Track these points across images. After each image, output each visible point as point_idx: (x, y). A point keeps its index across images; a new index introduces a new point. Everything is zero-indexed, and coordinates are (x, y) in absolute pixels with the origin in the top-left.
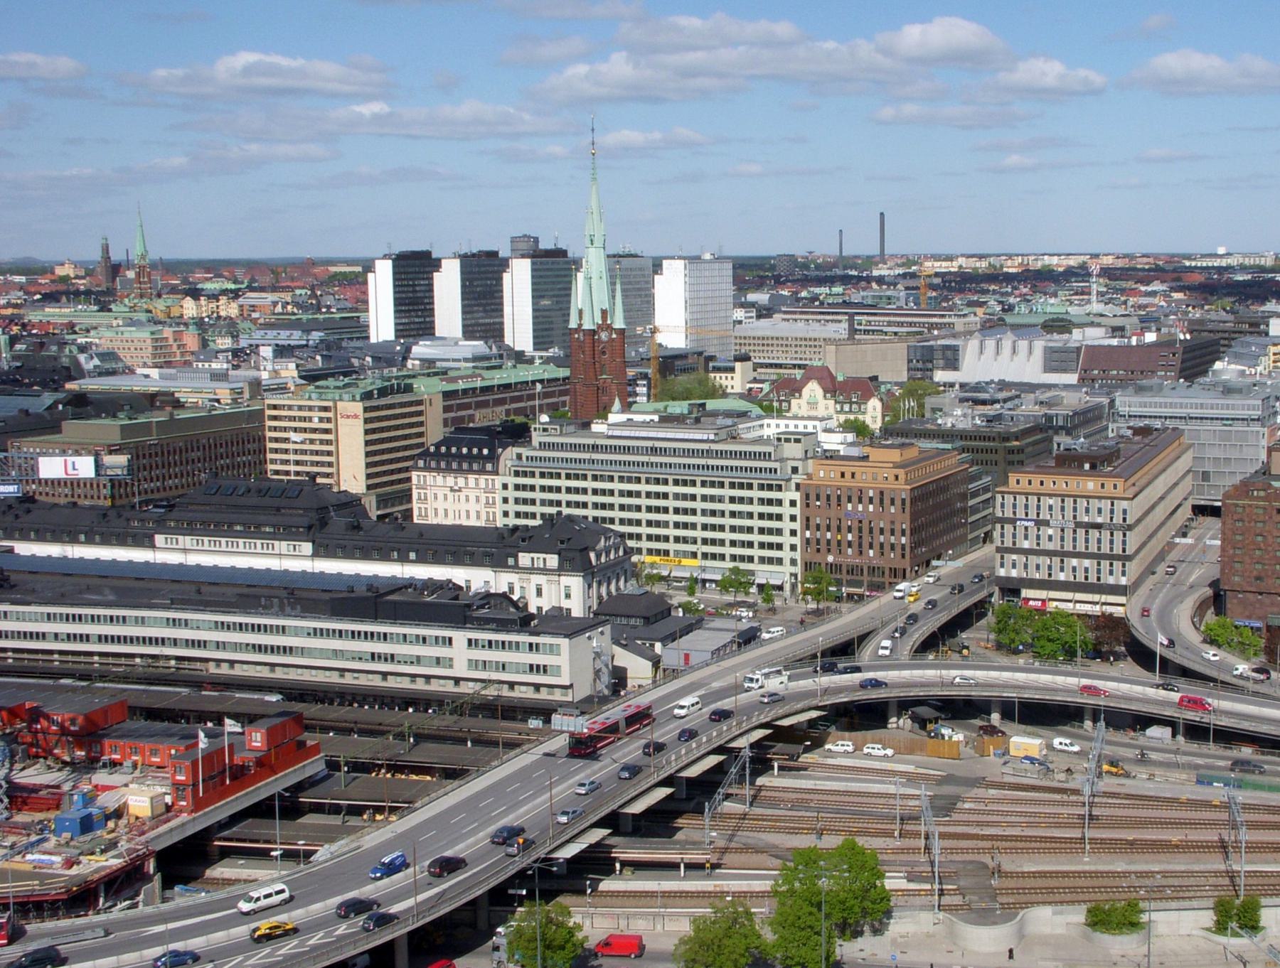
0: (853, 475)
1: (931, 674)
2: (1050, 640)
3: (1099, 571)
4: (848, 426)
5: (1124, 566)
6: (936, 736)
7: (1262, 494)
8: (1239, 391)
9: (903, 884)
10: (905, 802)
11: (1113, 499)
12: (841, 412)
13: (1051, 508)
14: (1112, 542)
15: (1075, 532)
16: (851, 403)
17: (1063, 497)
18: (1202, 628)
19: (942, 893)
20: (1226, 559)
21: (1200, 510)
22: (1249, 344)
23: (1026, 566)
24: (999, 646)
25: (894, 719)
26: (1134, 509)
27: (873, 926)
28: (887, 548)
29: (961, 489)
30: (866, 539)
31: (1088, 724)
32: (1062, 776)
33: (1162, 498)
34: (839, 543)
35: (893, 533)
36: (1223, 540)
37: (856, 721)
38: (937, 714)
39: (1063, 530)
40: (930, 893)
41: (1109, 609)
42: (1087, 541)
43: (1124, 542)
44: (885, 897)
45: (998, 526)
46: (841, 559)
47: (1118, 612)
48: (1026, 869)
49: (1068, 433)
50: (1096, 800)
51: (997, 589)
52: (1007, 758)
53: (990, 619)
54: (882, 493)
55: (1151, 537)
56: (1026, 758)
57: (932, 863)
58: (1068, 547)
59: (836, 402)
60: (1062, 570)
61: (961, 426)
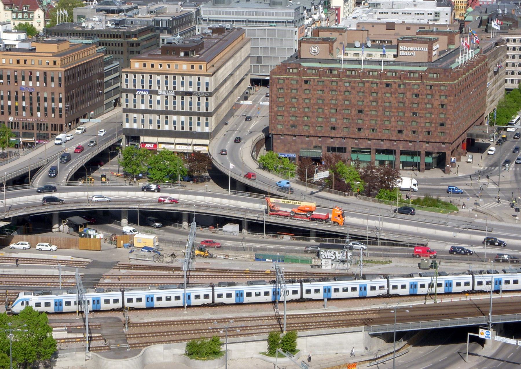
0: (25, 62)
1: (81, 195)
2: (160, 170)
3: (191, 124)
4: (21, 29)
5: (207, 120)
6: (85, 235)
9: (65, 335)
10: (65, 280)
11: (199, 76)
12: (16, 18)
13: (159, 82)
14: (199, 104)
15: (175, 98)
16: (23, 13)
17: (167, 75)
18: (258, 159)
19: (91, 339)
20: (273, 114)
21: (256, 82)
23: (143, 121)
24: (126, 175)
25: (56, 226)
26: (213, 82)
27: (45, 363)
28: (49, 111)
29: (99, 70)
30: (35, 106)
31: (185, 224)
32: (169, 259)
33: (231, 75)
34: (17, 108)
35: (53, 100)
36: (271, 102)
37: (31, 228)
38: (86, 221)
39: (167, 97)
40: (83, 339)
41: (198, 149)
42: (183, 104)
43: (207, 104)
44: (53, 344)
45: (124, 95)
46: (18, 119)
47: (204, 150)
48: (146, 321)
49: (170, 32)
50: (191, 273)
51: (124, 136)
52: (132, 248)
53: (119, 158)
54: (45, 74)
55: (224, 100)
56: (145, 248)
57: (84, 320)
58: (171, 108)
59: (13, 12)
60: (167, 123)
61: (100, 27)
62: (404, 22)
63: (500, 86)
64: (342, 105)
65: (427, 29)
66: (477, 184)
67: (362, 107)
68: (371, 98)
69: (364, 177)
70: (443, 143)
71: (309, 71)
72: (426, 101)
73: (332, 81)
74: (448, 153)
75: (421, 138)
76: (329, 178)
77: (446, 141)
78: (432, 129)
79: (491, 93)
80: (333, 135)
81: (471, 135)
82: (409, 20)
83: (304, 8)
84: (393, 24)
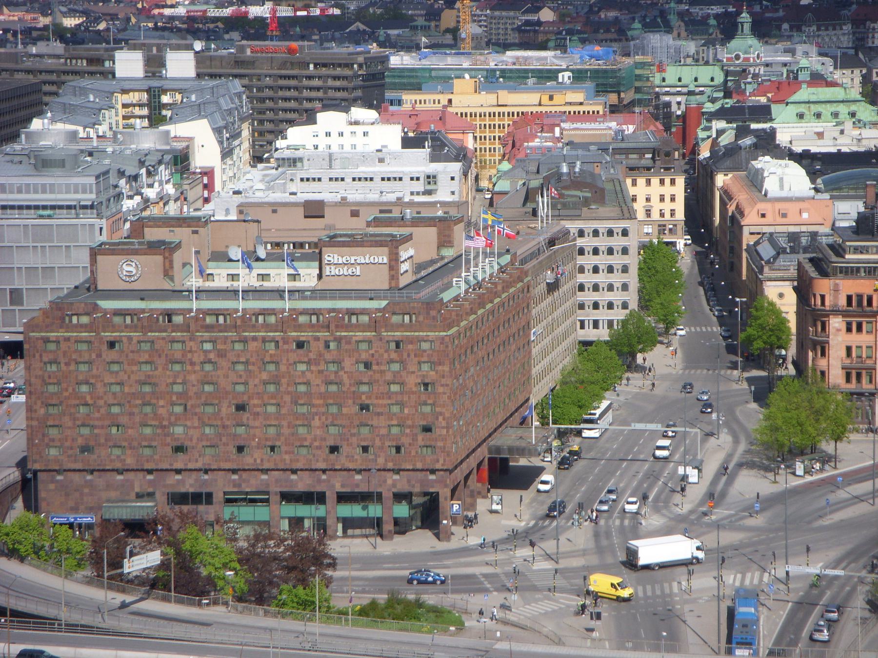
7: (85, 320)
8: (61, 164)
20: (35, 423)
22: (84, 91)
62: (344, 199)
63: (565, 335)
64: (198, 395)
65: (396, 214)
66: (509, 562)
67: (245, 398)
68: (264, 376)
69: (247, 560)
70: (433, 472)
71: (117, 320)
72: (389, 377)
73: (173, 341)
74: (444, 493)
75: (381, 461)
76: (164, 565)
77: (438, 466)
78: (406, 441)
79: (545, 353)
80: (179, 465)
81: (498, 450)
82: (356, 194)
83: (121, 174)
84: (320, 204)
